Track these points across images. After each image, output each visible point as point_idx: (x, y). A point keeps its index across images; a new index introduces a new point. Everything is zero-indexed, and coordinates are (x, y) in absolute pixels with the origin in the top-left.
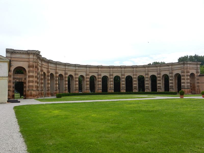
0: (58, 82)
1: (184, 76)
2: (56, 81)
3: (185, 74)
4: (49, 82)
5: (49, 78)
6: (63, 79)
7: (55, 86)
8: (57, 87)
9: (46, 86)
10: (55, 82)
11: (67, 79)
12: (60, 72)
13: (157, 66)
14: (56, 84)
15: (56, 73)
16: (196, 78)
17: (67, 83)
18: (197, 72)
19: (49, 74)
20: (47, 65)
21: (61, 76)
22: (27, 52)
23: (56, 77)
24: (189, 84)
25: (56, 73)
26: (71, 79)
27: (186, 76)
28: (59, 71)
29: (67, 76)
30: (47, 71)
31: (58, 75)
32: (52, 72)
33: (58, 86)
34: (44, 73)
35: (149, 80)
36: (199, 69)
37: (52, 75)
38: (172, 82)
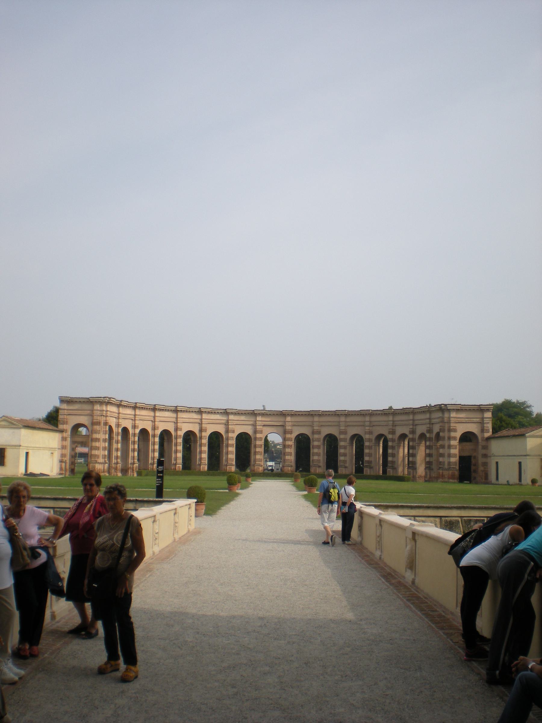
0: (136, 446)
1: (443, 438)
2: (134, 443)
3: (446, 434)
4: (119, 446)
5: (120, 438)
6: (148, 440)
7: (131, 454)
8: (134, 457)
9: (113, 454)
10: (131, 447)
11: (157, 440)
12: (141, 425)
13: (338, 414)
14: (134, 450)
15: (134, 427)
16: (481, 443)
17: (157, 447)
18: (483, 431)
19: (120, 430)
20: (117, 412)
21: (144, 432)
22: (90, 400)
23: (134, 435)
24: (455, 460)
25: (134, 427)
26: (166, 438)
27: (446, 438)
28: (141, 421)
29: (158, 432)
30: (116, 424)
31: (137, 431)
32: (128, 424)
33: (136, 454)
34: (110, 427)
35: (348, 447)
36: (488, 423)
37: (125, 430)
38: (431, 452)
